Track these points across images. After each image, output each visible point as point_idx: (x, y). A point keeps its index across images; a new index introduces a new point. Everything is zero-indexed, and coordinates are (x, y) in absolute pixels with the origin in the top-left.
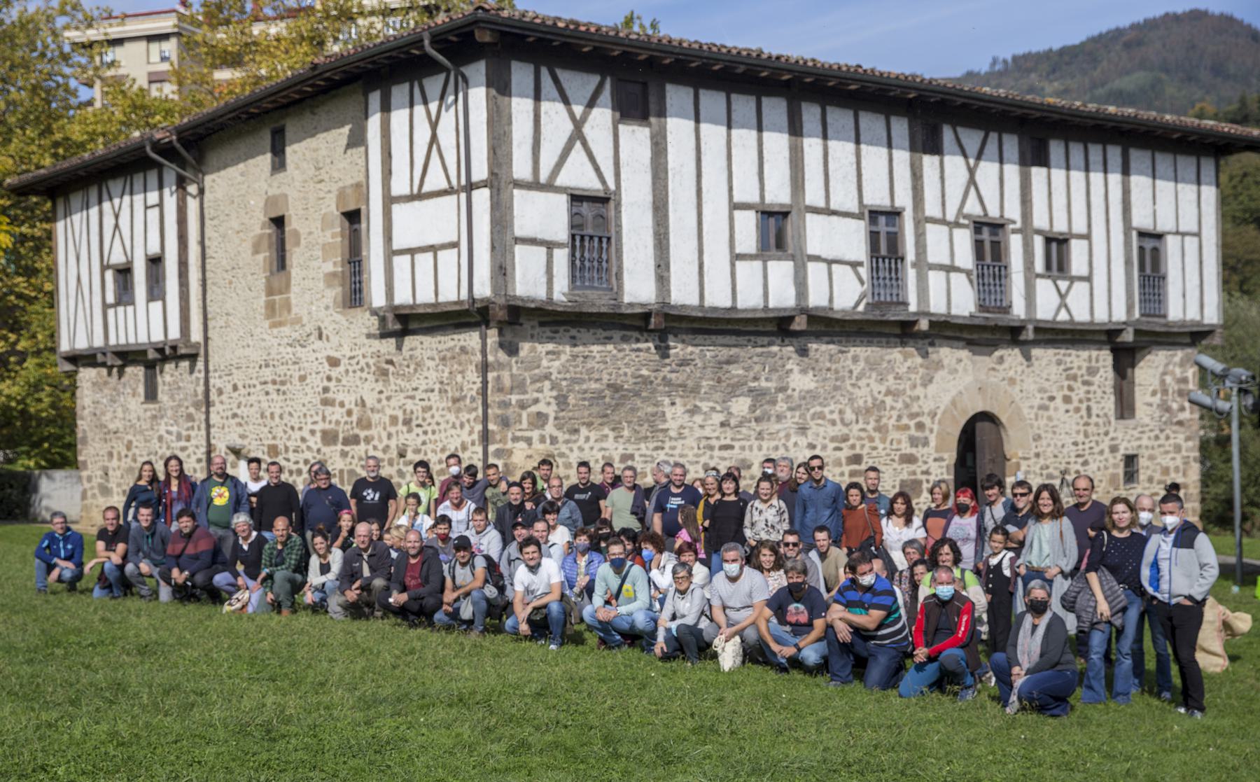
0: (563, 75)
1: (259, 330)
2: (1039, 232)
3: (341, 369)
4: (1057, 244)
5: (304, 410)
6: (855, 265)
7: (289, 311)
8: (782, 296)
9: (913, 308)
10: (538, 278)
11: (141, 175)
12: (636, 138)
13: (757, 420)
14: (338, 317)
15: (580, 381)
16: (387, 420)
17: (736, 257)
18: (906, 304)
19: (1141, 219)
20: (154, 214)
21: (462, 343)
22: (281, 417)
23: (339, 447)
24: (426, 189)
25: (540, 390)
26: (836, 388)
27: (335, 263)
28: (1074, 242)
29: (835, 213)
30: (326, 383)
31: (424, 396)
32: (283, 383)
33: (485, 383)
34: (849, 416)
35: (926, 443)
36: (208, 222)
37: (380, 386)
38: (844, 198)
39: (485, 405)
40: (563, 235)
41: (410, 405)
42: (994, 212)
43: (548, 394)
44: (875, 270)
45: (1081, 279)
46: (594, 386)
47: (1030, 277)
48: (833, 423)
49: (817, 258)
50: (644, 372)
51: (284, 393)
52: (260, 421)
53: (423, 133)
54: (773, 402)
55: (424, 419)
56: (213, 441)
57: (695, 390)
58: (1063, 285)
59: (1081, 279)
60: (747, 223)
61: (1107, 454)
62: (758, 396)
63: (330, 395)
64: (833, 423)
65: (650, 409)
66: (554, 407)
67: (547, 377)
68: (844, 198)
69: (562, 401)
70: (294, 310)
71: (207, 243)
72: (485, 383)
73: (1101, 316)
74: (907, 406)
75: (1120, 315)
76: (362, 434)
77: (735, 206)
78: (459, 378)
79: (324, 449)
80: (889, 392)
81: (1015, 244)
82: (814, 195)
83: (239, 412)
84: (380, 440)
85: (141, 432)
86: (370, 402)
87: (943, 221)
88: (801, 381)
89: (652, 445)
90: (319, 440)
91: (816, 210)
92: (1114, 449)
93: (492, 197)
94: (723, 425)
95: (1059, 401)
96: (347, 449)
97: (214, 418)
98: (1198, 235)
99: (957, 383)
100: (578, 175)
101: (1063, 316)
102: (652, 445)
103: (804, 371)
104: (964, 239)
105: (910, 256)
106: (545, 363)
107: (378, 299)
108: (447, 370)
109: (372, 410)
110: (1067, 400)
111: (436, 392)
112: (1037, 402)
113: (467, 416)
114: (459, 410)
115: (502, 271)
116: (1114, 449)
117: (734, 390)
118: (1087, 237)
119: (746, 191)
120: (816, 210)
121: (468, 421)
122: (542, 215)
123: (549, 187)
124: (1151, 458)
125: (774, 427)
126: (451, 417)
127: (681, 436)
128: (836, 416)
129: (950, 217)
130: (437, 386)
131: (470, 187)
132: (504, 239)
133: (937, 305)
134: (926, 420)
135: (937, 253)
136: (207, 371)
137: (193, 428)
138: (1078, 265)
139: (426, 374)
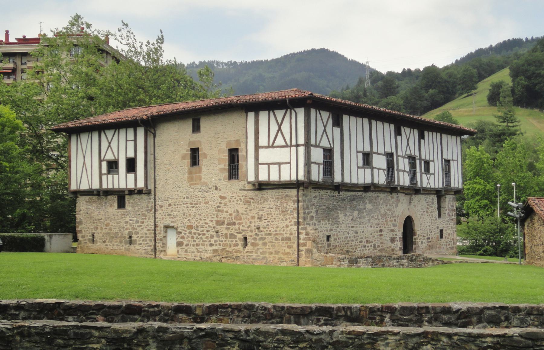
0: (321, 112)
1: (184, 186)
2: (423, 160)
3: (227, 200)
4: (427, 163)
5: (207, 213)
6: (384, 170)
7: (200, 180)
8: (368, 181)
9: (396, 183)
10: (317, 174)
11: (124, 130)
12: (337, 130)
13: (359, 218)
14: (226, 183)
15: (320, 206)
16: (250, 217)
17: (358, 168)
18: (395, 182)
19: (445, 157)
20: (131, 145)
21: (287, 193)
22: (195, 216)
23: (225, 226)
24: (275, 144)
25: (312, 209)
26: (377, 208)
27: (225, 165)
28: (431, 163)
29: (379, 154)
30: (218, 205)
31: (268, 210)
32: (196, 204)
33: (298, 206)
34: (380, 217)
35: (396, 226)
36: (156, 148)
37: (246, 206)
38: (381, 151)
39: (298, 214)
40: (322, 162)
41: (261, 213)
42: (413, 154)
43: (314, 210)
44: (388, 171)
45: (432, 174)
46: (324, 207)
48: (376, 219)
49: (376, 168)
50: (335, 203)
51: (196, 207)
52: (183, 217)
53: (274, 128)
54: (363, 213)
55: (268, 217)
56: (157, 224)
57: (346, 209)
58: (428, 176)
59: (432, 174)
60: (361, 156)
61: (436, 230)
62: (359, 210)
63: (221, 209)
64: (376, 219)
65: (336, 215)
66: (315, 214)
67: (314, 205)
69: (317, 212)
70: (203, 180)
71: (156, 155)
72: (298, 206)
73: (437, 186)
74: (392, 214)
75: (441, 186)
76: (237, 222)
77: (358, 152)
78: (285, 205)
79: (217, 227)
80: (388, 210)
81: (418, 162)
82: (375, 149)
83: (172, 213)
84: (246, 223)
85: (115, 220)
86: (241, 211)
87: (402, 156)
88: (369, 206)
89: (336, 226)
90: (214, 224)
91: (375, 153)
92: (438, 228)
93: (305, 149)
94: (352, 220)
95: (425, 212)
96: (229, 227)
97: (157, 215)
98: (457, 161)
100: (325, 143)
101: (428, 186)
102: (336, 226)
103: (370, 203)
104: (407, 161)
105: (396, 168)
106: (313, 200)
107: (251, 177)
108: (279, 202)
109: (242, 214)
110: (427, 212)
111: (274, 209)
112: (421, 213)
113: (288, 217)
114: (285, 215)
115: (308, 172)
116: (438, 228)
118: (433, 161)
119: (360, 149)
120: (375, 153)
121: (289, 218)
122: (317, 155)
123: (318, 146)
124: (446, 230)
125: (364, 220)
126: (281, 217)
127: (343, 223)
128: (376, 217)
129: (404, 155)
130: (274, 207)
131: (297, 145)
132: (308, 163)
133: (402, 183)
134: (396, 218)
135: (401, 167)
136: (155, 199)
137: (145, 219)
138: (432, 171)
139: (269, 203)
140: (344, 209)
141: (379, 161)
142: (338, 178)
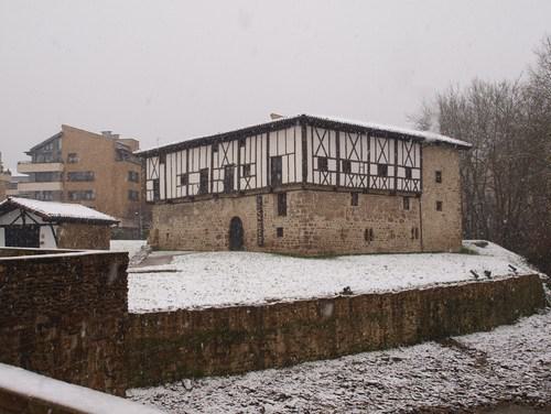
4: (247, 168)
19: (273, 153)
47: (239, 177)
60: (179, 178)
68: (196, 169)
82: (190, 170)
88: (196, 212)
99: (228, 210)
100: (155, 177)
117: (184, 215)
135: (215, 177)
140: (178, 216)
141: (195, 179)
142: (162, 197)
